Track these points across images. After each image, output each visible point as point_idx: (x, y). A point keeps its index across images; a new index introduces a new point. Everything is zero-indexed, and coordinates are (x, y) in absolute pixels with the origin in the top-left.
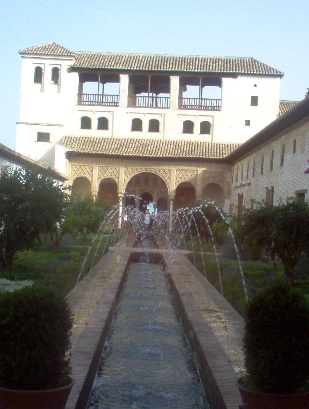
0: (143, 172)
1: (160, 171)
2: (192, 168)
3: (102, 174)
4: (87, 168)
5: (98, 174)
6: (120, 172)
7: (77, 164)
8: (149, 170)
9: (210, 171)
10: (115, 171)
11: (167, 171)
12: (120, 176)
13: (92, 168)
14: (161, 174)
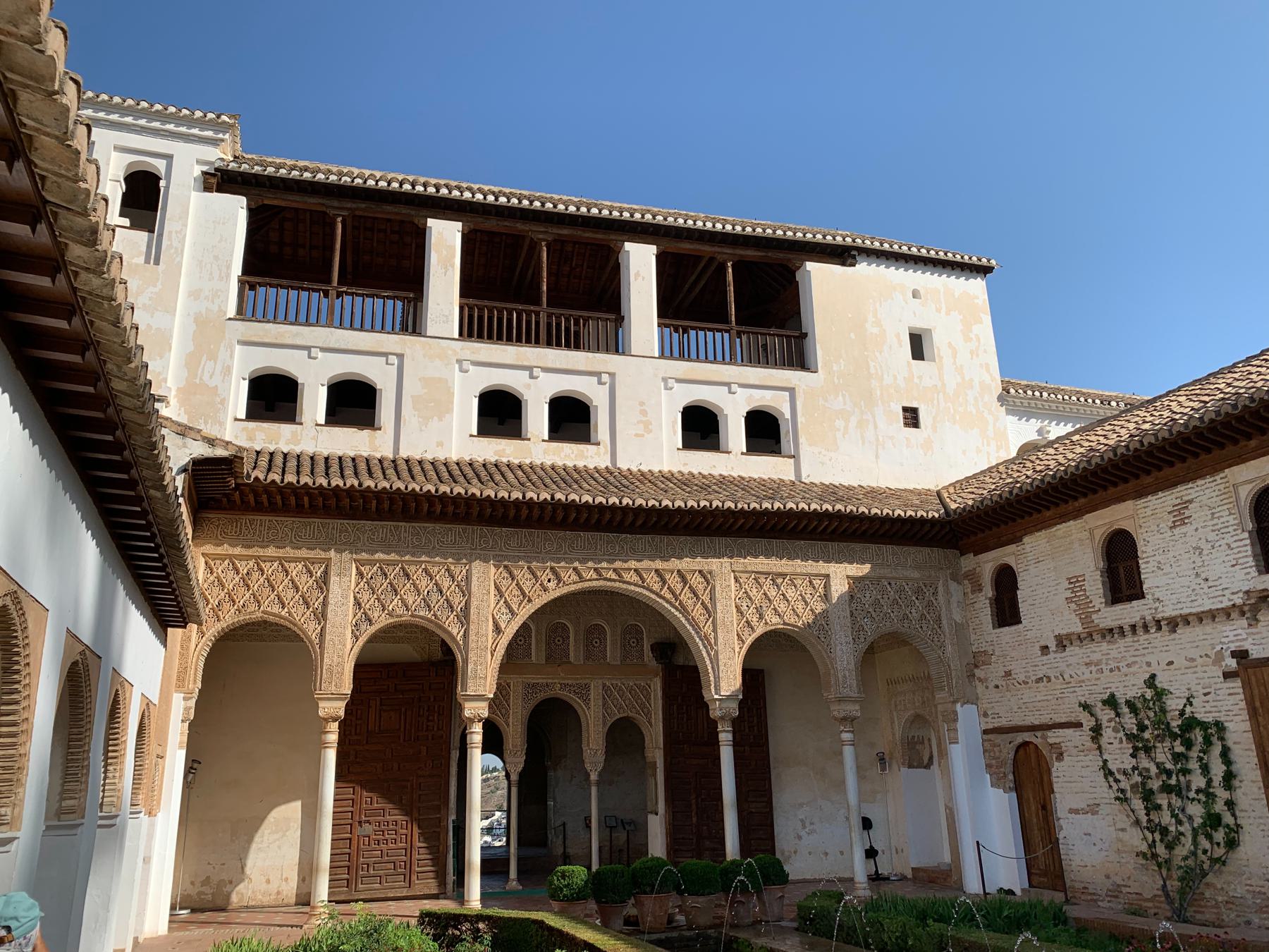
0: (587, 584)
1: (664, 582)
2: (798, 566)
3: (378, 599)
4: (295, 569)
5: (358, 603)
6: (474, 589)
7: (238, 550)
8: (614, 576)
9: (879, 579)
10: (446, 583)
11: (696, 580)
12: (473, 610)
13: (326, 573)
14: (669, 596)
